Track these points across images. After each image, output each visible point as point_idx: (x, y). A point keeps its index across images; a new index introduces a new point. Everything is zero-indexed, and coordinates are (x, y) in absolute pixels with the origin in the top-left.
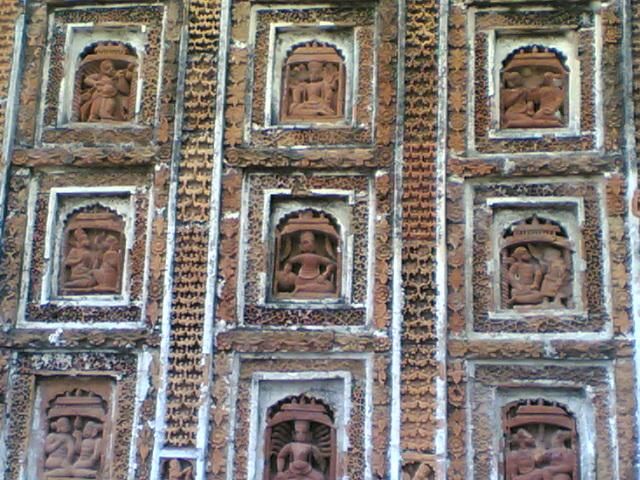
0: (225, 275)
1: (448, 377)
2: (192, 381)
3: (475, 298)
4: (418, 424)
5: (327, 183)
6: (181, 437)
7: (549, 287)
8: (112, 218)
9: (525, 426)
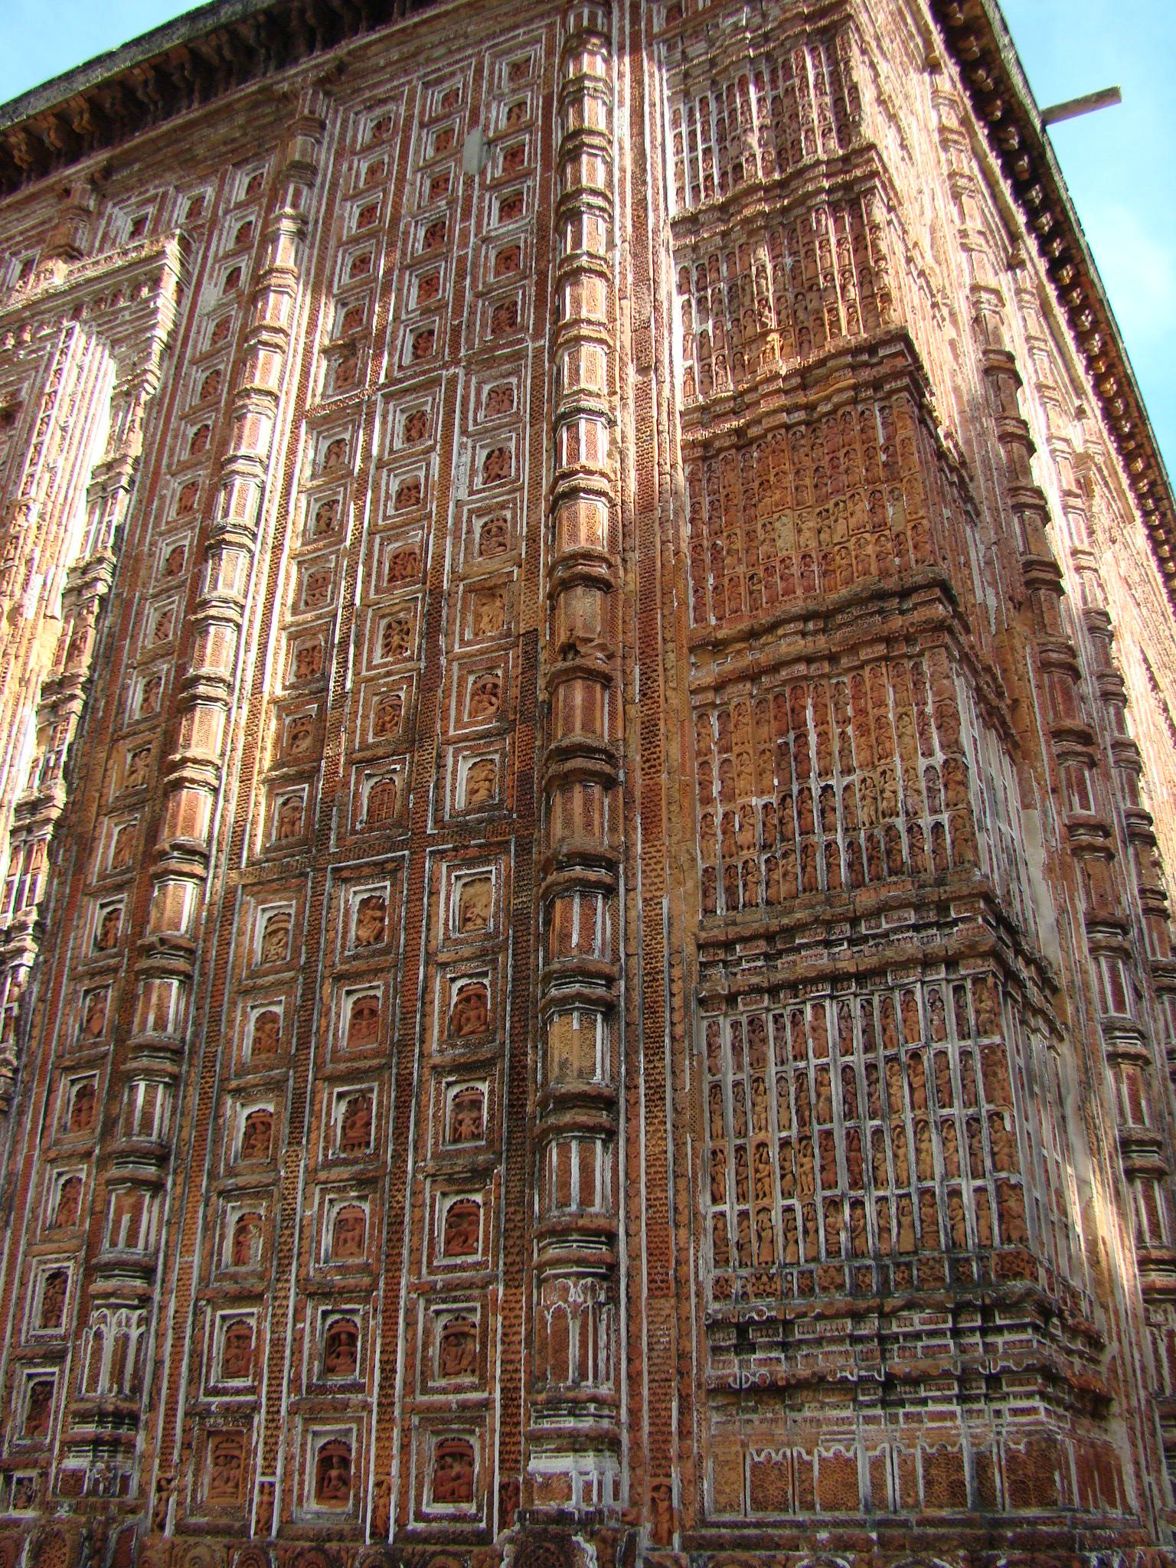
0: (296, 1364)
5: (350, 1301)
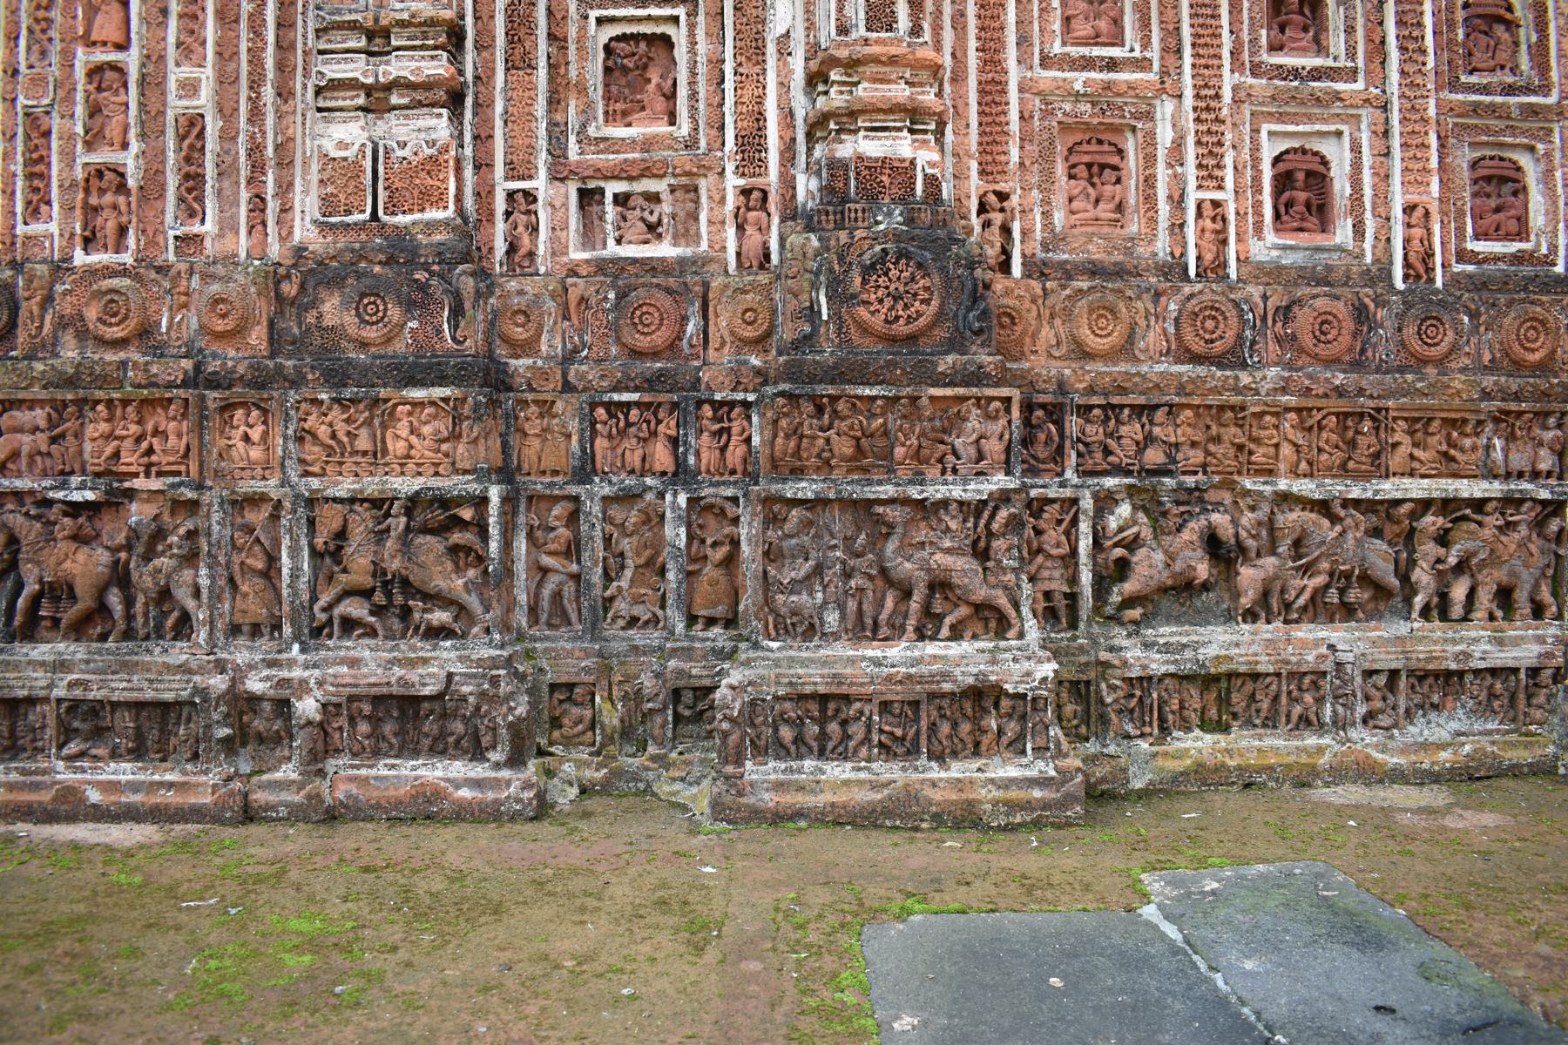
7: (1502, 56)
9: (1482, 178)
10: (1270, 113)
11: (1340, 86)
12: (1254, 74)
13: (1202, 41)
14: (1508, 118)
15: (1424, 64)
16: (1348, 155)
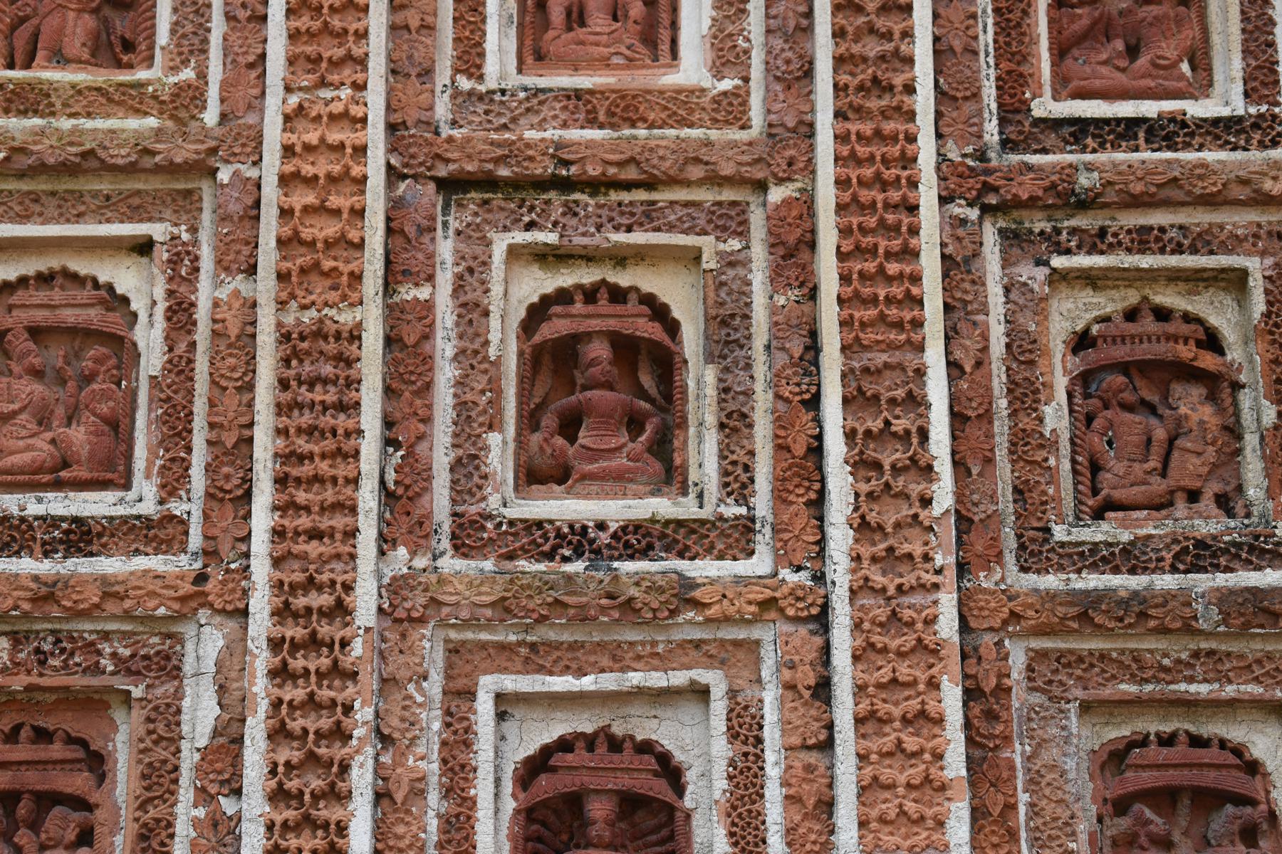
1: (966, 676)
2: (332, 694)
3: (1019, 492)
4: (901, 791)
5: (649, 217)
6: (307, 832)
7: (1188, 467)
8: (102, 302)
9: (1147, 795)
10: (503, 647)
11: (703, 569)
12: (460, 549)
13: (306, 470)
14: (1189, 629)
15: (926, 502)
16: (721, 749)
